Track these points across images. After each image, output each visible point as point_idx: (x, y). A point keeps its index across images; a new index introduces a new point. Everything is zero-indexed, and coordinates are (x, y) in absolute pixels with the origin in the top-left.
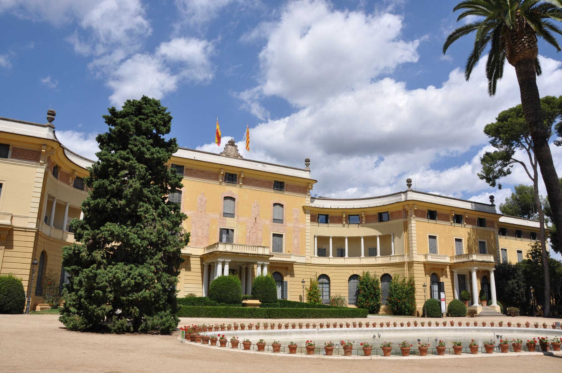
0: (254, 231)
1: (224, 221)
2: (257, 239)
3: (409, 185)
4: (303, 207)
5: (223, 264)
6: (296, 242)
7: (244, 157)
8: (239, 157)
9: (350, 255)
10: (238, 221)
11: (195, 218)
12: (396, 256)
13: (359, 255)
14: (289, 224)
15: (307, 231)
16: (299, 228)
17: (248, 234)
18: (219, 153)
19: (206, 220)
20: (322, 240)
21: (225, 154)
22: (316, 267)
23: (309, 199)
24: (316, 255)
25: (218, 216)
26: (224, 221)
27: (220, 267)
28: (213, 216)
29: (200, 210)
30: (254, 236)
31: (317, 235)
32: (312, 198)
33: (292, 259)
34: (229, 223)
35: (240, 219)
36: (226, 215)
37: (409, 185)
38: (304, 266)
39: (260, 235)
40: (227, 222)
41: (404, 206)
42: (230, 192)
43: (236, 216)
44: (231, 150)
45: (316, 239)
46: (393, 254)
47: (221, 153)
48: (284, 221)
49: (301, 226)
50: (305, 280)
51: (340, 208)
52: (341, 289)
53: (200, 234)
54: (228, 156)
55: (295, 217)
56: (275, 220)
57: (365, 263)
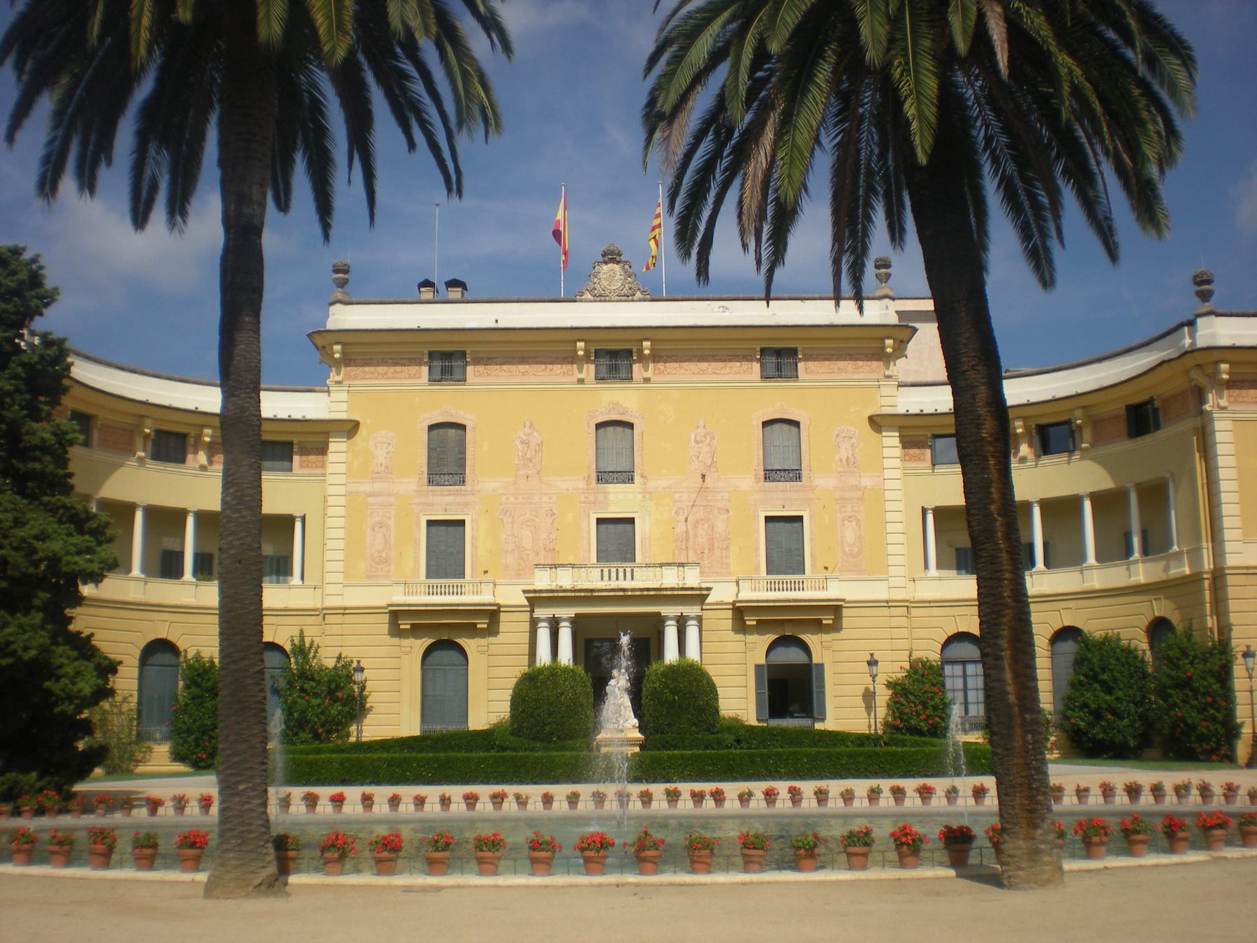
1: (601, 497)
6: (850, 535)
10: (645, 493)
11: (512, 499)
13: (1075, 558)
14: (822, 477)
16: (857, 488)
17: (681, 528)
19: (545, 499)
22: (936, 611)
25: (582, 485)
26: (601, 497)
27: (544, 635)
29: (523, 472)
30: (700, 532)
31: (930, 505)
33: (833, 592)
34: (619, 500)
35: (652, 484)
36: (603, 477)
38: (886, 611)
39: (720, 527)
40: (611, 497)
41: (1187, 372)
43: (637, 478)
44: (611, 279)
45: (930, 518)
48: (804, 473)
49: (867, 482)
50: (876, 657)
51: (1033, 400)
53: (527, 543)
55: (844, 452)
56: (770, 475)
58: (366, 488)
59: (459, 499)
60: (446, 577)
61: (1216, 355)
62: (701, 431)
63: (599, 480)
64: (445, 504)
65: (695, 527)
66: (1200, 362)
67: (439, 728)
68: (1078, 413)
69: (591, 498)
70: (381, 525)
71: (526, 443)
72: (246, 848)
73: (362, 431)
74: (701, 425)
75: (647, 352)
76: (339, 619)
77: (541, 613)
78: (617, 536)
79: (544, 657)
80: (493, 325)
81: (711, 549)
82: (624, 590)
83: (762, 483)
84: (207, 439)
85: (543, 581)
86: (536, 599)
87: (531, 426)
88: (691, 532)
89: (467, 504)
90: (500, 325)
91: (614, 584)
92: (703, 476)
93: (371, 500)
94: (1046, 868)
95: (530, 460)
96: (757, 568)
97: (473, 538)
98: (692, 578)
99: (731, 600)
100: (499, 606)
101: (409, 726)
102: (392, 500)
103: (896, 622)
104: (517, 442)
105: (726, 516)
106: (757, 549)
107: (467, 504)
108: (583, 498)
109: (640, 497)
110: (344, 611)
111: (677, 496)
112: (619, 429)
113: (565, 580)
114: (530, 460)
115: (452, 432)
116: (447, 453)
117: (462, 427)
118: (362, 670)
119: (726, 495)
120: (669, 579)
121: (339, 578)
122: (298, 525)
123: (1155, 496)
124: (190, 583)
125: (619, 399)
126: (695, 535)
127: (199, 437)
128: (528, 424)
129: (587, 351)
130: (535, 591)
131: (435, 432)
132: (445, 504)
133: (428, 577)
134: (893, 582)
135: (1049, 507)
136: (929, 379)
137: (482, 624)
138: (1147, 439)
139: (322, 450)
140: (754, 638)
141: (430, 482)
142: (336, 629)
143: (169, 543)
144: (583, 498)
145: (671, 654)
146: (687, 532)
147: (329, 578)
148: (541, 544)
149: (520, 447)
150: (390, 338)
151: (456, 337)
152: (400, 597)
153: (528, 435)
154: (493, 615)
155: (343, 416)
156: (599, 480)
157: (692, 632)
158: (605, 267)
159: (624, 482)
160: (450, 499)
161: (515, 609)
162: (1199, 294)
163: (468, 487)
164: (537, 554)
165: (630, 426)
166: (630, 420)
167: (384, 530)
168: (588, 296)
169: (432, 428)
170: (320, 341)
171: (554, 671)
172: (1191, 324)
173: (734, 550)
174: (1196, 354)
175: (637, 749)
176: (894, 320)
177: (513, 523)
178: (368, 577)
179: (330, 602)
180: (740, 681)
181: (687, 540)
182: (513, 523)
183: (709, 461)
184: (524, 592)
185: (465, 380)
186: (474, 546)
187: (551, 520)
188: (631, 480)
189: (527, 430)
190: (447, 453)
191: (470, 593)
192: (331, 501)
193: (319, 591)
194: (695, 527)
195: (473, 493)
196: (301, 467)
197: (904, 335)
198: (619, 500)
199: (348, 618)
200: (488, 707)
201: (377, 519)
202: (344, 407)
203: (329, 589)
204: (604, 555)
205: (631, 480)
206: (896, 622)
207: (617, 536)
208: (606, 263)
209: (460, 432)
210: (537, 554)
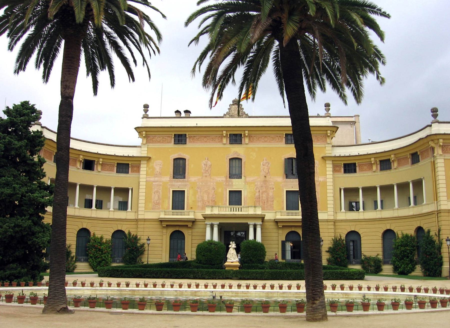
0: (264, 190)
2: (267, 198)
3: (435, 116)
4: (323, 158)
5: (212, 226)
7: (250, 115)
8: (244, 116)
9: (400, 206)
10: (245, 182)
11: (201, 183)
12: (428, 204)
15: (328, 184)
17: (257, 194)
18: (222, 115)
19: (212, 184)
20: (350, 192)
21: (229, 115)
23: (331, 148)
24: (343, 210)
25: (224, 179)
26: (230, 183)
27: (208, 230)
28: (219, 179)
29: (205, 175)
30: (264, 195)
32: (333, 146)
34: (237, 184)
35: (248, 179)
36: (231, 176)
37: (435, 116)
38: (327, 223)
39: (271, 194)
40: (234, 183)
42: (236, 153)
45: (342, 191)
46: (425, 202)
47: (225, 115)
51: (378, 152)
52: (371, 247)
53: (206, 198)
54: (232, 116)
57: (400, 215)
58: (152, 179)
60: (178, 209)
61: (438, 137)
62: (265, 161)
63: (230, 177)
64: (178, 185)
65: (262, 194)
66: (432, 139)
67: (175, 260)
68: (392, 156)
69: (227, 184)
70: (157, 192)
71: (206, 165)
72: (56, 298)
73: (152, 160)
74: (265, 159)
75: (247, 135)
76: (143, 223)
77: (208, 222)
78: (235, 197)
79: (208, 238)
80: (196, 125)
81: (267, 202)
82: (236, 215)
83: (285, 179)
84: (101, 163)
85: (208, 212)
86: (206, 217)
87: (208, 159)
88: (261, 196)
89: (186, 185)
90: (198, 125)
91: (232, 213)
92: (265, 177)
93: (154, 183)
94: (320, 314)
96: (283, 209)
98: (259, 212)
99: (273, 219)
100: (196, 219)
101: (165, 258)
102: (161, 183)
103: (330, 227)
104: (203, 165)
105: (272, 191)
106: (283, 202)
107: (186, 185)
108: (224, 184)
109: (244, 183)
110: (145, 220)
111: (256, 183)
112: (237, 161)
113: (216, 211)
115: (181, 161)
116: (179, 168)
117: (185, 159)
118: (150, 240)
119: (273, 183)
120: (251, 212)
121: (143, 209)
122: (130, 191)
123: (418, 184)
124: (94, 210)
125: (237, 150)
126: (262, 197)
127: (98, 161)
129: (227, 135)
130: (205, 215)
131: (175, 161)
132: (178, 185)
133: (172, 209)
134: (329, 213)
135: (383, 188)
136: (345, 144)
137: (190, 224)
138: (416, 165)
139: (139, 167)
140: (280, 231)
141: (174, 178)
142: (142, 226)
143: (88, 197)
144: (224, 184)
145: (251, 237)
146: (259, 195)
147: (140, 209)
150: (161, 129)
151: (183, 129)
152: (163, 216)
153: (207, 162)
154: (194, 222)
155: (146, 155)
156: (230, 177)
157: (259, 230)
158: (233, 106)
159: (238, 178)
160: (180, 183)
161: (200, 221)
162: (432, 116)
163: (186, 180)
165: (241, 159)
166: (241, 157)
167: (158, 193)
168: (228, 116)
169: (174, 159)
170: (139, 130)
171: (211, 243)
172: (431, 126)
173: (275, 202)
174: (431, 136)
175: (238, 269)
176: (331, 124)
177: (201, 192)
178: (153, 209)
179: (140, 217)
180: (277, 246)
181: (260, 198)
182: (201, 192)
183: (267, 172)
184: (202, 215)
185: (186, 144)
186: (187, 199)
188: (241, 177)
189: (206, 160)
190: (179, 168)
191: (187, 215)
192: (141, 183)
193: (136, 213)
194: (262, 194)
195: (188, 181)
196: (132, 172)
197: (334, 129)
198: (237, 184)
199: (146, 223)
200: (190, 253)
201: (156, 190)
202: (146, 152)
203: (140, 213)
204: (231, 203)
205: (241, 177)
206: (330, 227)
207: (235, 197)
208: (233, 105)
210: (209, 202)
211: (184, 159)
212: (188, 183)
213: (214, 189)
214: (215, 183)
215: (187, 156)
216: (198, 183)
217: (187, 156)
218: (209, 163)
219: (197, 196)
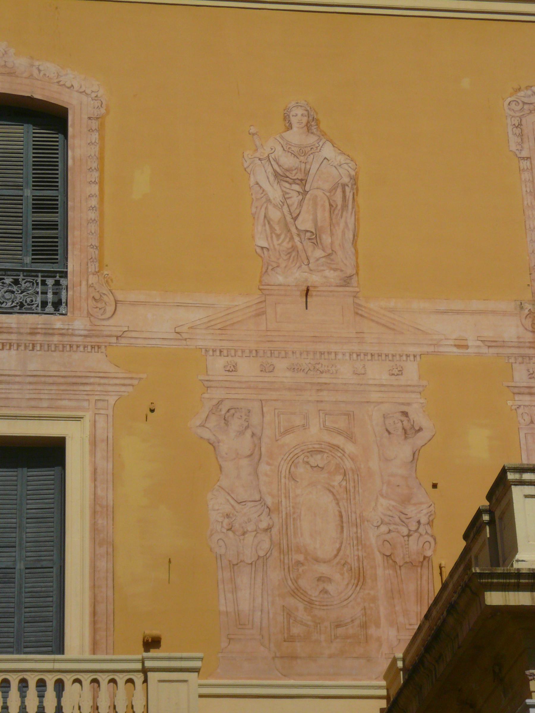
11: (248, 368)
19: (377, 372)
25: (512, 329)
29: (297, 276)
53: (318, 533)
59: (36, 363)
95: (315, 238)
97: (98, 508)
104: (262, 176)
108: (520, 376)
114: (315, 238)
115: (19, 137)
128: (298, 117)
144: (520, 376)
148: (372, 537)
149: (274, 192)
153: (303, 152)
164: (360, 577)
182: (255, 456)
186: (98, 538)
187: (403, 451)
189: (296, 136)
195: (95, 342)
209: (45, 134)
210: (360, 577)
211: (51, 118)
212: (96, 361)
213: (410, 431)
214: (412, 372)
215: (70, 77)
216: (218, 364)
217: (70, 77)
218: (330, 163)
219: (217, 504)
